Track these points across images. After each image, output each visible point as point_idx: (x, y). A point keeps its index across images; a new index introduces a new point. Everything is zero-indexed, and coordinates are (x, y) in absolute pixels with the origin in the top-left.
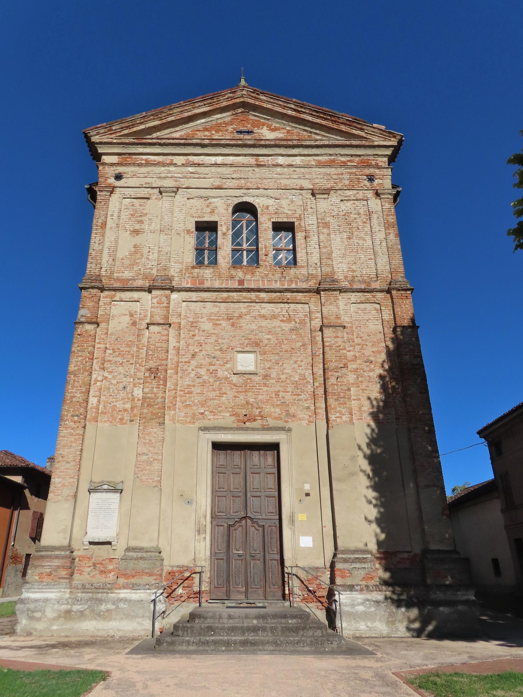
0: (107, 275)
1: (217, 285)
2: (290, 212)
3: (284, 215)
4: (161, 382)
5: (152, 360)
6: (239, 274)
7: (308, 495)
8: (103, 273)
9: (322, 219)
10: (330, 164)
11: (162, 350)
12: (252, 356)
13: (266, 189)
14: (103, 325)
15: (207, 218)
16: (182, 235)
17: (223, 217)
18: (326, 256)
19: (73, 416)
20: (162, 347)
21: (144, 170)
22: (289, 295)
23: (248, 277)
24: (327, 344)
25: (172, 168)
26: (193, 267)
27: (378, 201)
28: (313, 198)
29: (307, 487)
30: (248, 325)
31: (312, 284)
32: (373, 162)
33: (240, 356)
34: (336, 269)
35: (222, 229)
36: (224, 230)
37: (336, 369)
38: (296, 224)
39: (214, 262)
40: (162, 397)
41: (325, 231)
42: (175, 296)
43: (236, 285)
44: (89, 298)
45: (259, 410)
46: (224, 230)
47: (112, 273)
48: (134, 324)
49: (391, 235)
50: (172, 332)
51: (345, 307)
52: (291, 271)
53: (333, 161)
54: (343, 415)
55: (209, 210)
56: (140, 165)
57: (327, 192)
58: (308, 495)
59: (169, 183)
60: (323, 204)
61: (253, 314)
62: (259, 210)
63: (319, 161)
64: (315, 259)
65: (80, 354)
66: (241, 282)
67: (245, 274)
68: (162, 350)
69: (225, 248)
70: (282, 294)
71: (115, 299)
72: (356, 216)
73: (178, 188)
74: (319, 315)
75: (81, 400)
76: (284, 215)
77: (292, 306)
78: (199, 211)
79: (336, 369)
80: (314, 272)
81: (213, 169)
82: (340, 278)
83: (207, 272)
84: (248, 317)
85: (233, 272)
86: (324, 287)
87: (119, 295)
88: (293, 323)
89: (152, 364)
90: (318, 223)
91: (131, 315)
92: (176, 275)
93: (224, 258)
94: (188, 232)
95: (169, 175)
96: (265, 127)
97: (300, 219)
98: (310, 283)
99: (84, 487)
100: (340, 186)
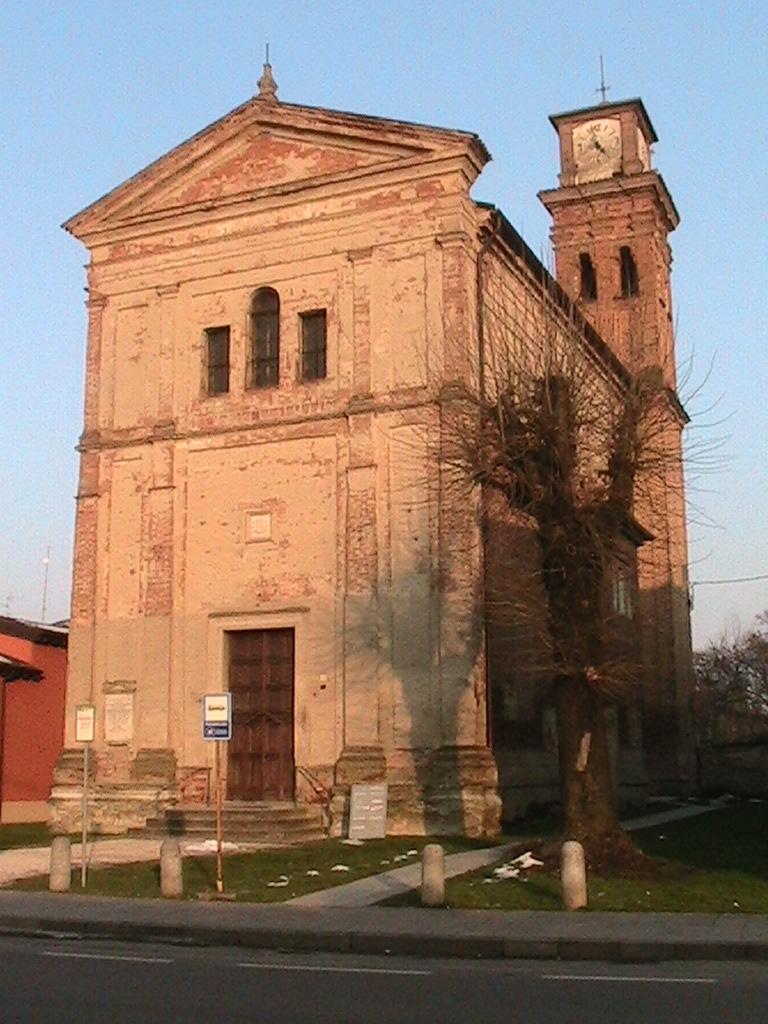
3: (314, 300)
5: (155, 536)
7: (323, 687)
8: (102, 426)
9: (361, 299)
10: (376, 203)
12: (267, 517)
13: (289, 263)
16: (186, 352)
17: (237, 317)
18: (363, 358)
19: (82, 611)
21: (138, 263)
22: (311, 425)
25: (172, 255)
26: (201, 402)
27: (439, 254)
28: (349, 264)
31: (341, 405)
32: (437, 186)
33: (254, 518)
35: (235, 336)
38: (328, 312)
40: (168, 582)
41: (363, 318)
42: (181, 445)
43: (251, 423)
45: (275, 588)
48: (138, 489)
52: (318, 388)
53: (377, 197)
55: (219, 309)
56: (132, 257)
57: (368, 251)
58: (323, 687)
59: (169, 279)
60: (365, 272)
62: (280, 294)
63: (362, 202)
66: (255, 415)
69: (238, 365)
70: (305, 426)
71: (116, 458)
73: (178, 285)
75: (87, 593)
76: (314, 300)
80: (346, 386)
83: (218, 405)
88: (317, 464)
89: (156, 542)
90: (355, 306)
91: (135, 479)
92: (181, 415)
96: (292, 153)
97: (332, 303)
99: (99, 687)
100: (386, 239)
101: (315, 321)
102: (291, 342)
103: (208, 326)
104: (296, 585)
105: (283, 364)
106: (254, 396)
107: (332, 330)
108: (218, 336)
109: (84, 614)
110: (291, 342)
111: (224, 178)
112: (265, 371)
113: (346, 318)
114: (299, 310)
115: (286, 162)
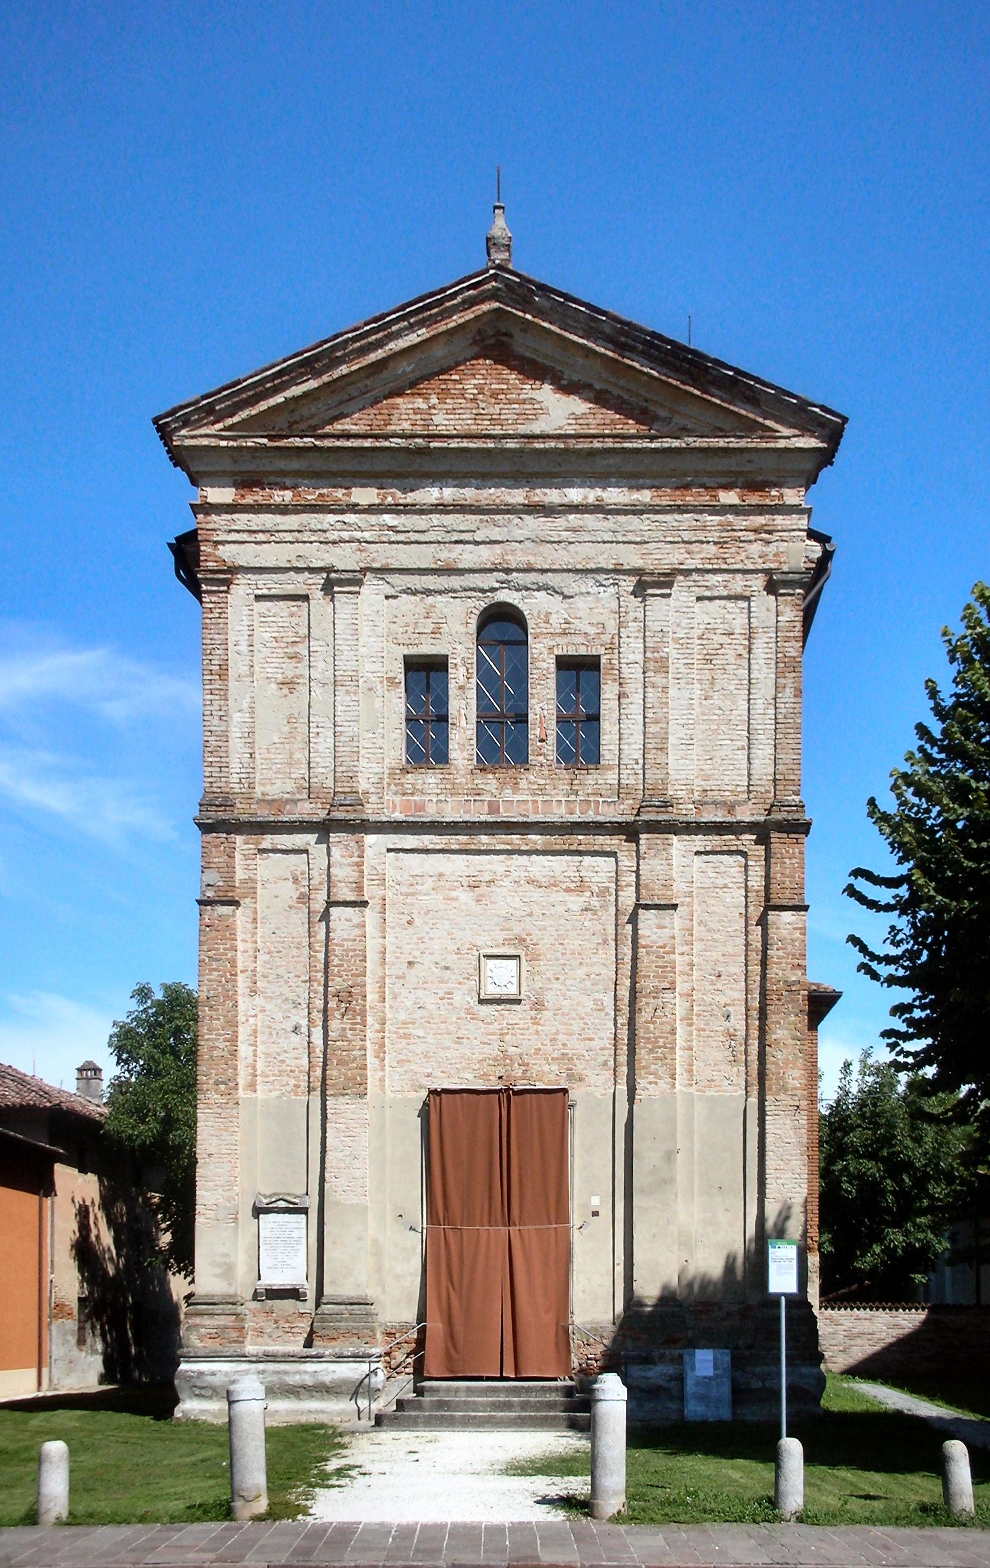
0: (243, 790)
1: (452, 814)
2: (592, 630)
4: (359, 1019)
6: (490, 782)
7: (595, 1214)
9: (656, 650)
11: (356, 956)
14: (246, 902)
15: (427, 648)
17: (458, 641)
18: (655, 745)
19: (217, 1083)
20: (355, 950)
23: (508, 794)
24: (642, 942)
26: (405, 771)
29: (595, 1201)
30: (507, 899)
34: (673, 775)
36: (462, 680)
37: (656, 992)
38: (603, 661)
39: (442, 757)
41: (658, 679)
42: (370, 839)
44: (216, 847)
46: (462, 680)
47: (252, 786)
49: (788, 690)
50: (370, 915)
51: (678, 862)
54: (661, 1078)
58: (595, 1214)
61: (515, 875)
62: (531, 624)
64: (633, 752)
65: (215, 965)
66: (493, 808)
67: (502, 785)
68: (356, 956)
72: (725, 640)
74: (633, 878)
76: (580, 639)
77: (588, 860)
78: (410, 629)
79: (656, 992)
81: (436, 519)
82: (681, 794)
83: (430, 779)
84: (506, 882)
85: (479, 780)
86: (646, 824)
87: (268, 841)
88: (588, 894)
90: (646, 660)
93: (462, 747)
94: (391, 681)
95: (345, 535)
98: (622, 807)
101: (580, 671)
102: (543, 702)
103: (413, 651)
104: (555, 1067)
105: (534, 733)
106: (490, 776)
107: (609, 692)
108: (425, 672)
109: (222, 1087)
110: (543, 702)
111: (434, 400)
112: (504, 738)
113: (633, 674)
114: (558, 652)
115: (537, 395)
